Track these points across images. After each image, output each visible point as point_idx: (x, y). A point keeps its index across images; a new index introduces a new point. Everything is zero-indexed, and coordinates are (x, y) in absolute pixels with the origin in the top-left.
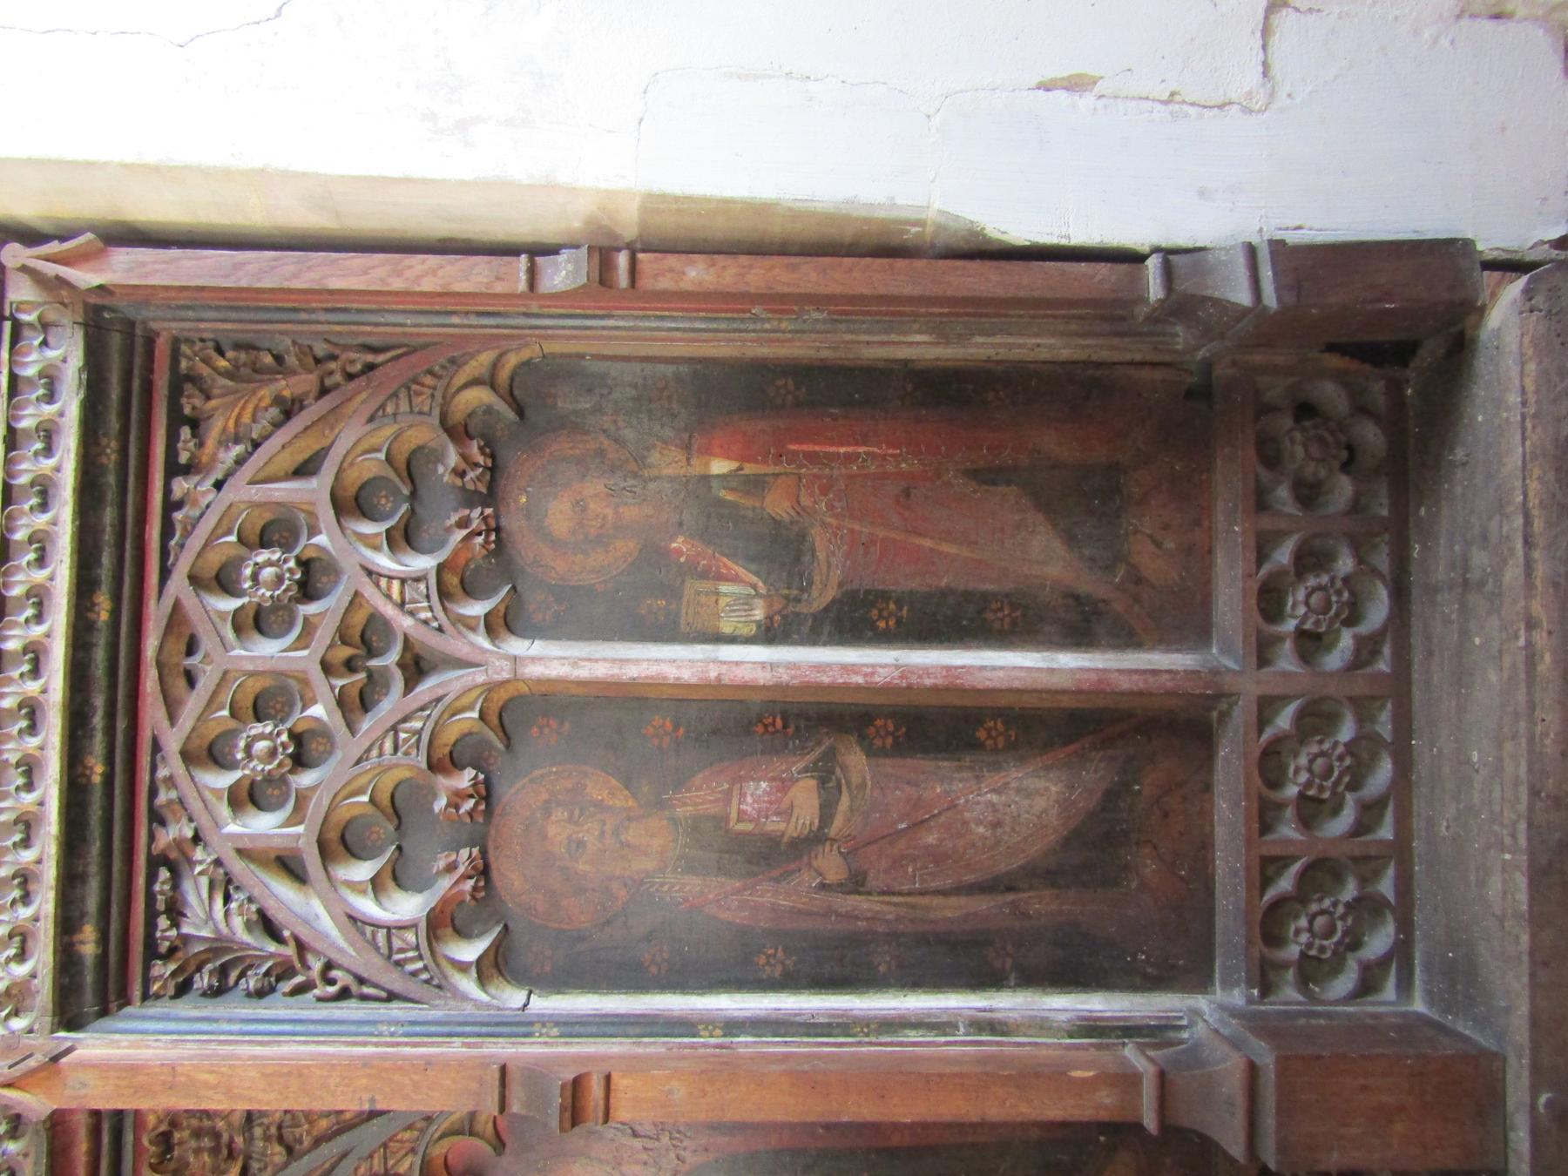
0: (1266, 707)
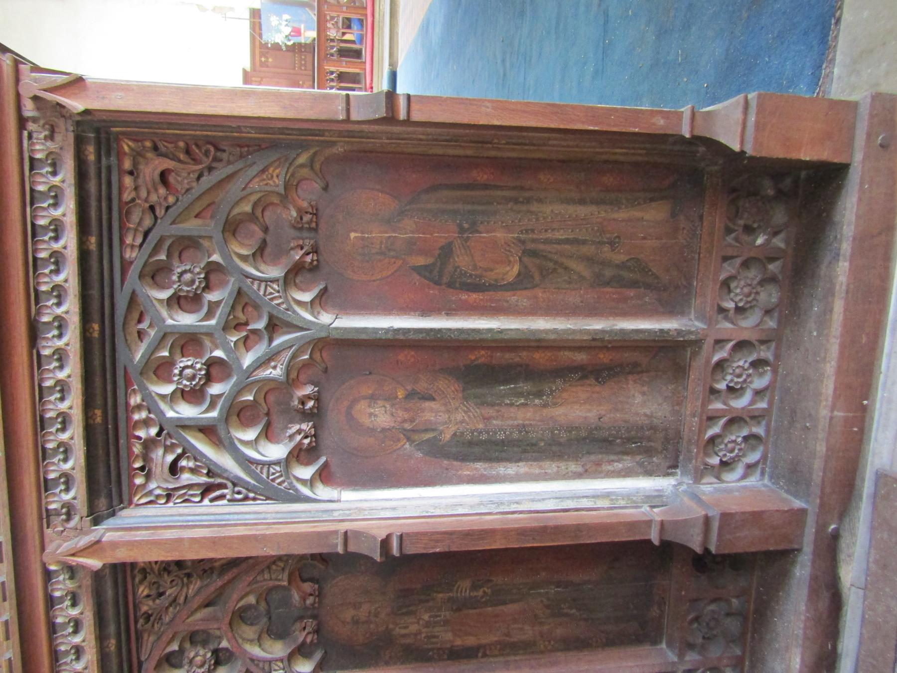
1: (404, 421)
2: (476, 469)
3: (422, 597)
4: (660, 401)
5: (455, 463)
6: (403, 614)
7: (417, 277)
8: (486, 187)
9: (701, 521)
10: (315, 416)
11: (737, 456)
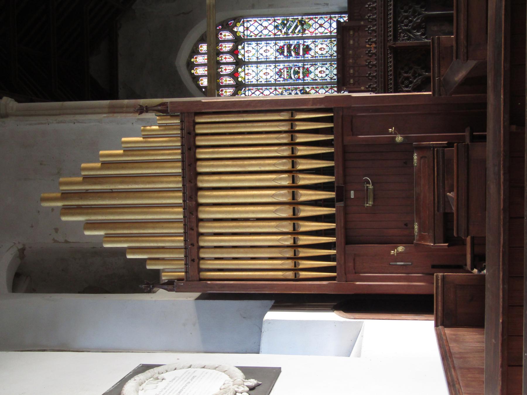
10: (425, 28)
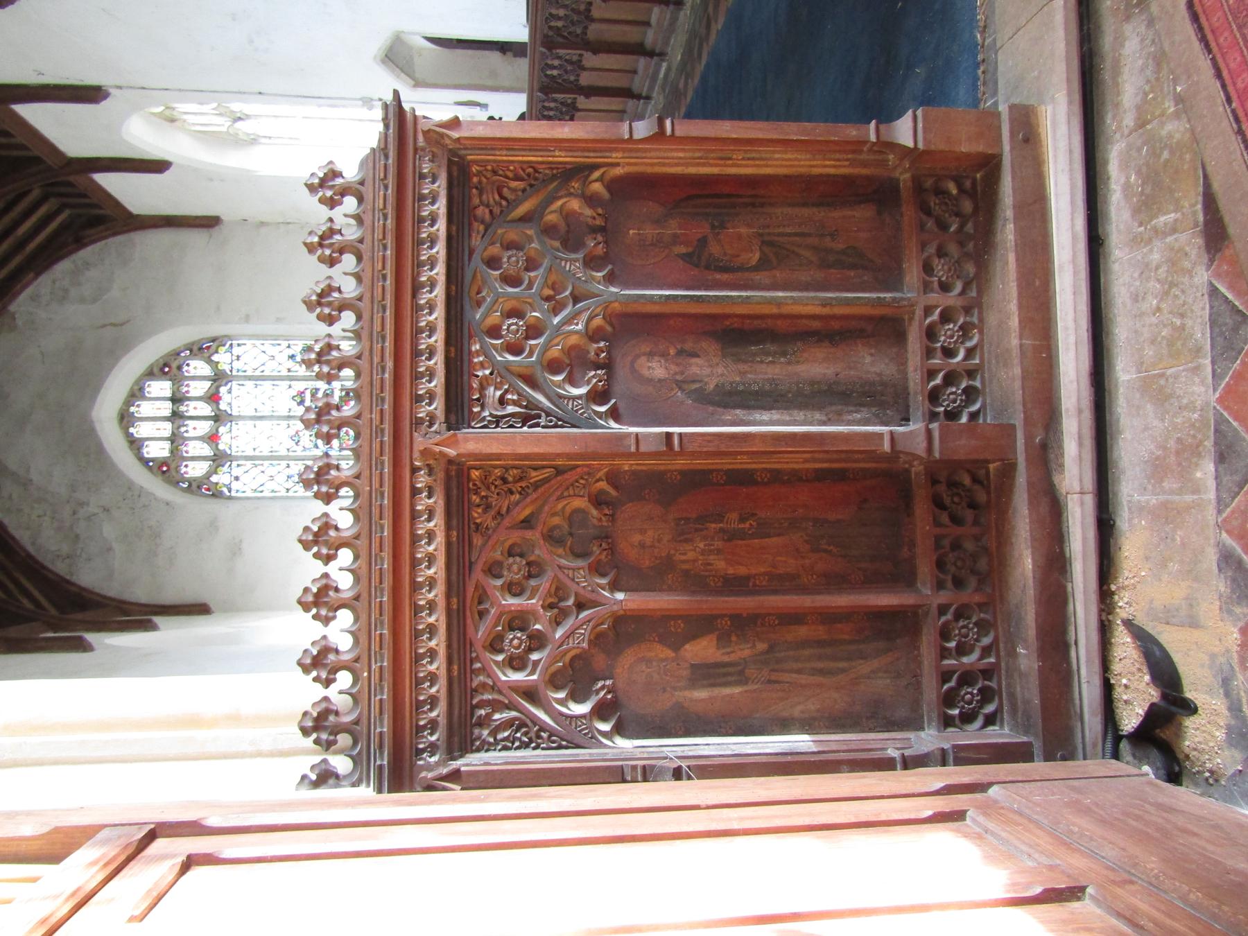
0: (928, 311)
1: (676, 374)
2: (736, 415)
3: (697, 526)
4: (887, 361)
5: (718, 409)
6: (680, 541)
7: (681, 262)
8: (729, 196)
9: (923, 430)
10: (608, 366)
11: (959, 406)
